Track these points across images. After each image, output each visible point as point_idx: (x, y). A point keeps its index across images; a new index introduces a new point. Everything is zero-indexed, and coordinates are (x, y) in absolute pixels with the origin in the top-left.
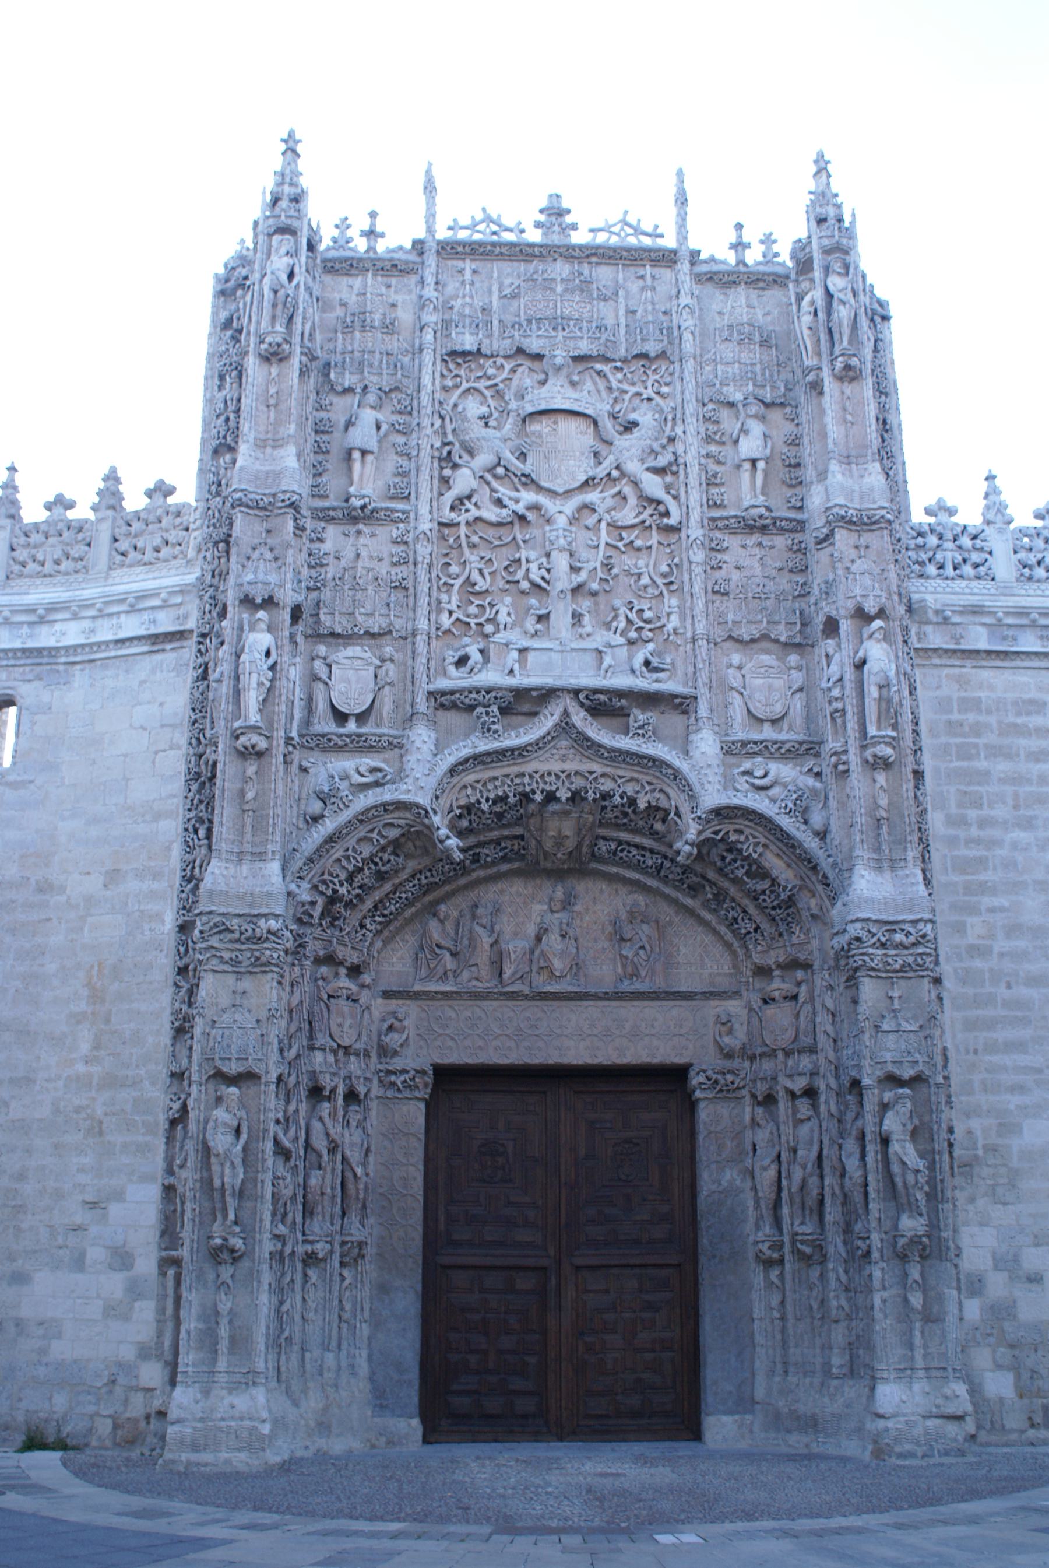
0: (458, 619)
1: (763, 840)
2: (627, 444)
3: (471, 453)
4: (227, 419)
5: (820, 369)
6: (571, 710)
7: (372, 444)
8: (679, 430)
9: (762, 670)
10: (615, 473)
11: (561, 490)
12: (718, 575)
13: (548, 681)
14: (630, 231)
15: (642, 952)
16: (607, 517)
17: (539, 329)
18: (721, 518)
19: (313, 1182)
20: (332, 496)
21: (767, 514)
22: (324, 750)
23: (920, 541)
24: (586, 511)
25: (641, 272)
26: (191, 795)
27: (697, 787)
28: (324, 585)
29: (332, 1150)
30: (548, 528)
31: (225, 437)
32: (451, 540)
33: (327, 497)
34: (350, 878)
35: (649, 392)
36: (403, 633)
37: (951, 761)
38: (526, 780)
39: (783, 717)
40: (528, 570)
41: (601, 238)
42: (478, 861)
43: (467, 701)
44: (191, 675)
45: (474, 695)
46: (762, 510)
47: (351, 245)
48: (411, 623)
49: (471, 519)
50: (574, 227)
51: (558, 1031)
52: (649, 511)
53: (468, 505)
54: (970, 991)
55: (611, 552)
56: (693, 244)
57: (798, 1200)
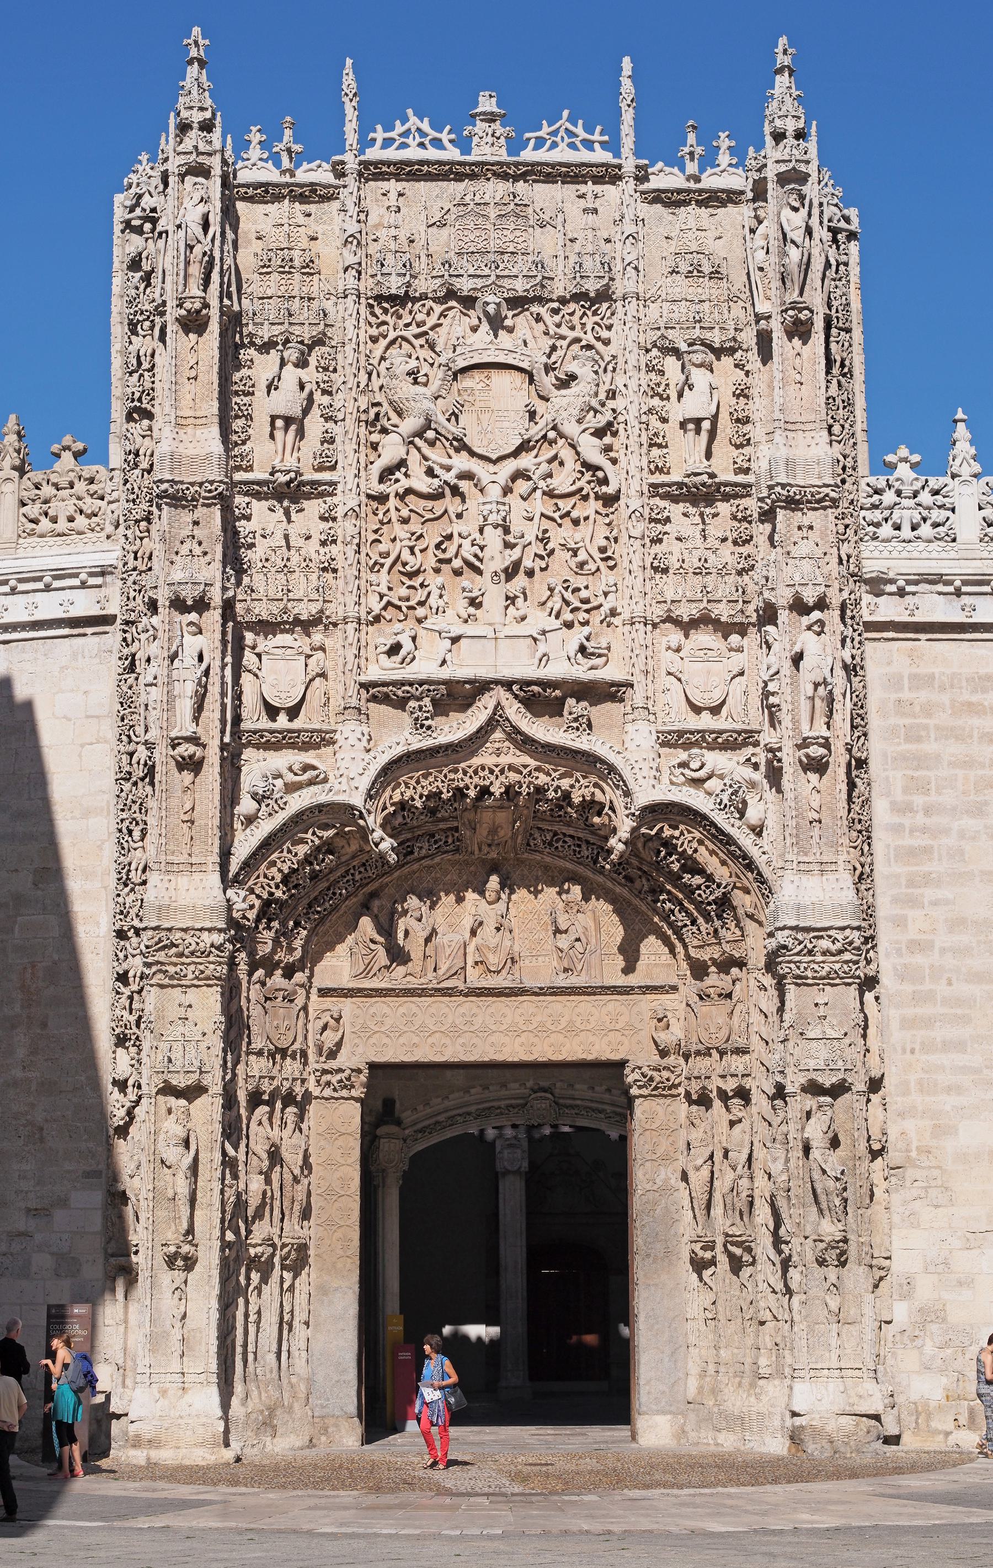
2: (565, 401)
3: (400, 414)
6: (504, 703)
10: (552, 435)
11: (494, 457)
12: (657, 548)
16: (542, 484)
18: (663, 485)
22: (258, 747)
24: (520, 481)
25: (583, 188)
26: (123, 794)
27: (631, 784)
31: (140, 400)
32: (381, 516)
33: (251, 466)
34: (286, 880)
35: (589, 338)
36: (333, 620)
38: (460, 775)
40: (460, 546)
43: (400, 693)
44: (115, 666)
45: (407, 688)
49: (401, 491)
52: (588, 476)
55: (546, 524)
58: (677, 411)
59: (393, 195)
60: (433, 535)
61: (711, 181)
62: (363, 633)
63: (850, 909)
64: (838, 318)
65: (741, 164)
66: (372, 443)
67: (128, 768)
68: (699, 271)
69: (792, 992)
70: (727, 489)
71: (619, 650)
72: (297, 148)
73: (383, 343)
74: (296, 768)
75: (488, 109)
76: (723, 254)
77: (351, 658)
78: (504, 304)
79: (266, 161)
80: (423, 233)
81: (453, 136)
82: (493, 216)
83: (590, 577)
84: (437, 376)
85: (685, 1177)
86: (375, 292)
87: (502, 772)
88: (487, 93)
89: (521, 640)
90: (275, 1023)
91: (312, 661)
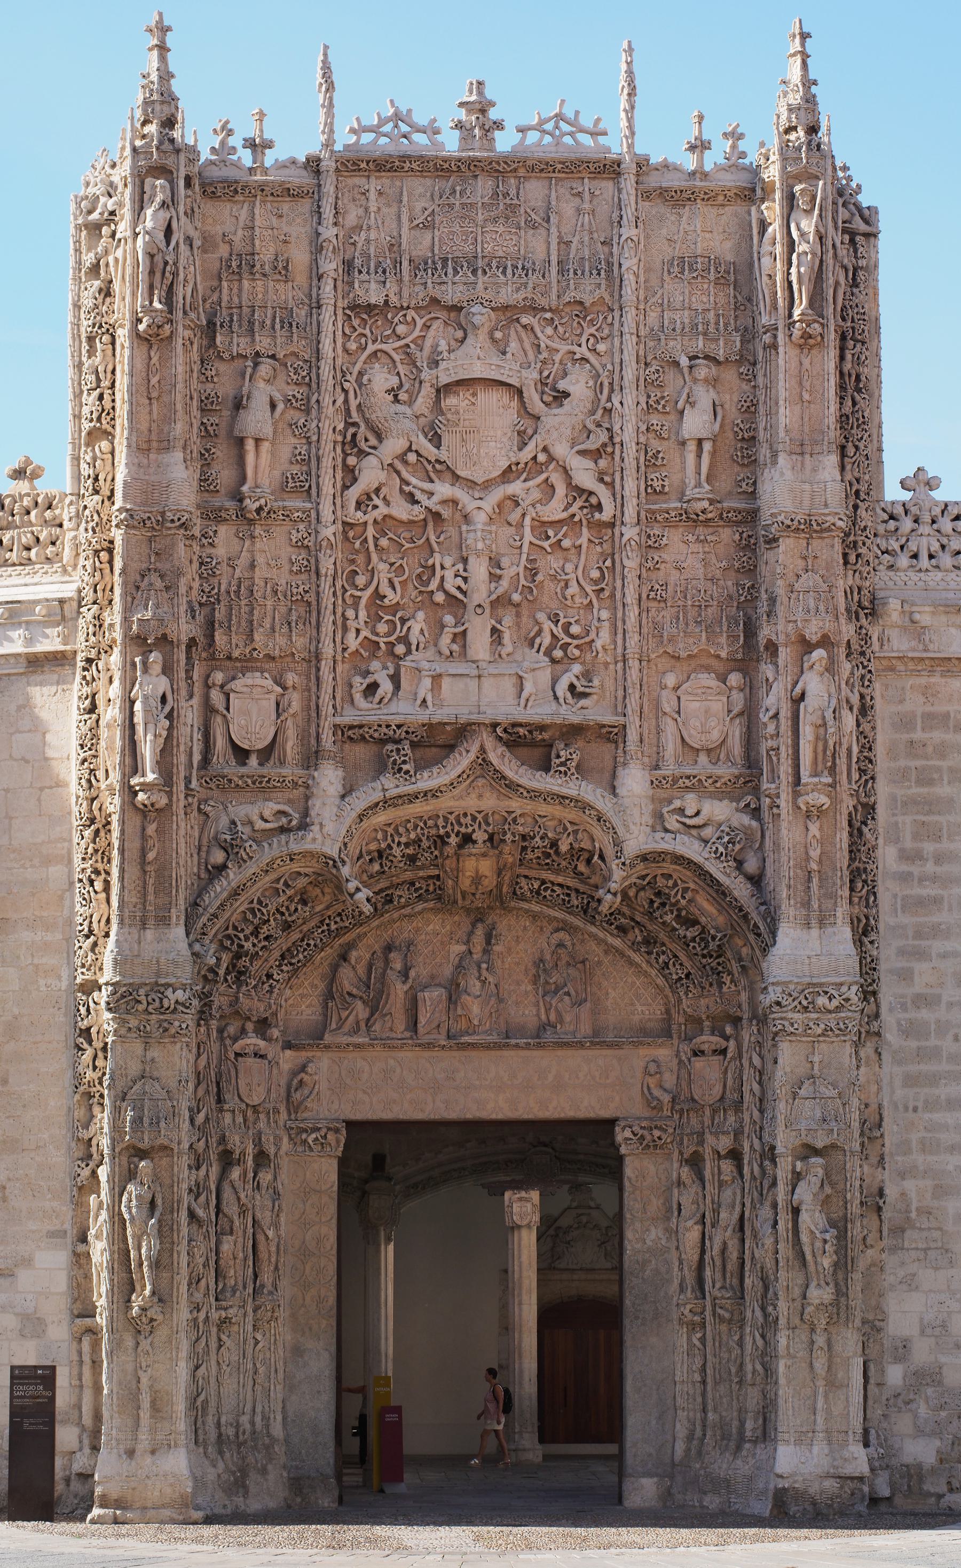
1: (692, 886)
4: (101, 398)
5: (777, 329)
7: (267, 430)
8: (616, 400)
9: (700, 691)
14: (565, 127)
17: (456, 272)
18: (661, 511)
19: (226, 1247)
27: (621, 831)
28: (219, 601)
30: (464, 528)
31: (99, 419)
34: (256, 933)
35: (583, 351)
37: (910, 787)
40: (442, 578)
41: (533, 137)
43: (376, 735)
45: (384, 730)
46: (705, 504)
47: (235, 157)
48: (314, 643)
49: (379, 518)
50: (499, 125)
52: (579, 503)
53: (376, 501)
54: (913, 1044)
56: (639, 150)
57: (718, 1262)
60: (411, 566)
74: (267, 814)
87: (486, 818)
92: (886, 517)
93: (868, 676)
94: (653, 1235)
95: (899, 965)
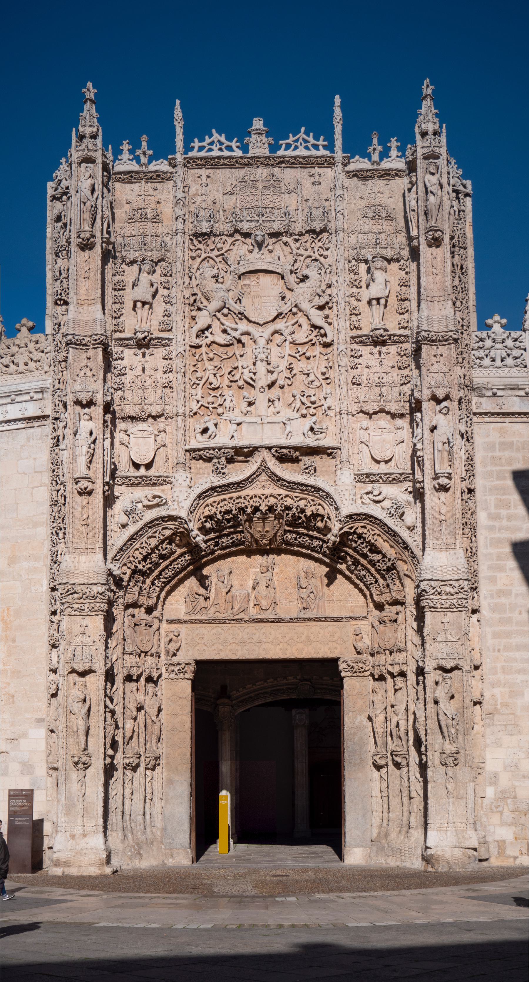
0: (202, 405)
1: (377, 532)
2: (302, 290)
4: (62, 282)
6: (267, 459)
7: (149, 298)
10: (295, 310)
11: (261, 323)
12: (355, 372)
13: (255, 442)
15: (312, 595)
16: (289, 338)
20: (126, 330)
21: (384, 333)
22: (128, 485)
23: (481, 343)
25: (312, 171)
26: (53, 514)
27: (339, 503)
29: (140, 708)
31: (61, 294)
34: (145, 559)
35: (316, 255)
36: (170, 415)
37: (493, 481)
39: (391, 460)
42: (218, 545)
43: (208, 455)
44: (50, 442)
45: (211, 452)
46: (382, 331)
49: (209, 343)
51: (265, 640)
54: (497, 616)
55: (292, 360)
58: (365, 295)
59: (204, 178)
61: (386, 164)
62: (188, 422)
63: (463, 569)
64: (459, 241)
65: (403, 155)
66: (192, 317)
67: (56, 499)
68: (379, 216)
69: (429, 617)
70: (395, 338)
71: (333, 429)
72: (150, 152)
73: (199, 260)
74: (150, 497)
75: (258, 127)
76: (393, 206)
77: (180, 436)
78: (266, 236)
79: (132, 160)
80: (221, 198)
81: (238, 144)
82: (260, 187)
83: (317, 390)
84: (229, 279)
85: (370, 719)
86: (194, 232)
88: (258, 119)
89: (277, 424)
90: (140, 638)
91: (158, 438)
92: (478, 340)
93: (470, 422)
94: (359, 720)
95: (489, 574)
